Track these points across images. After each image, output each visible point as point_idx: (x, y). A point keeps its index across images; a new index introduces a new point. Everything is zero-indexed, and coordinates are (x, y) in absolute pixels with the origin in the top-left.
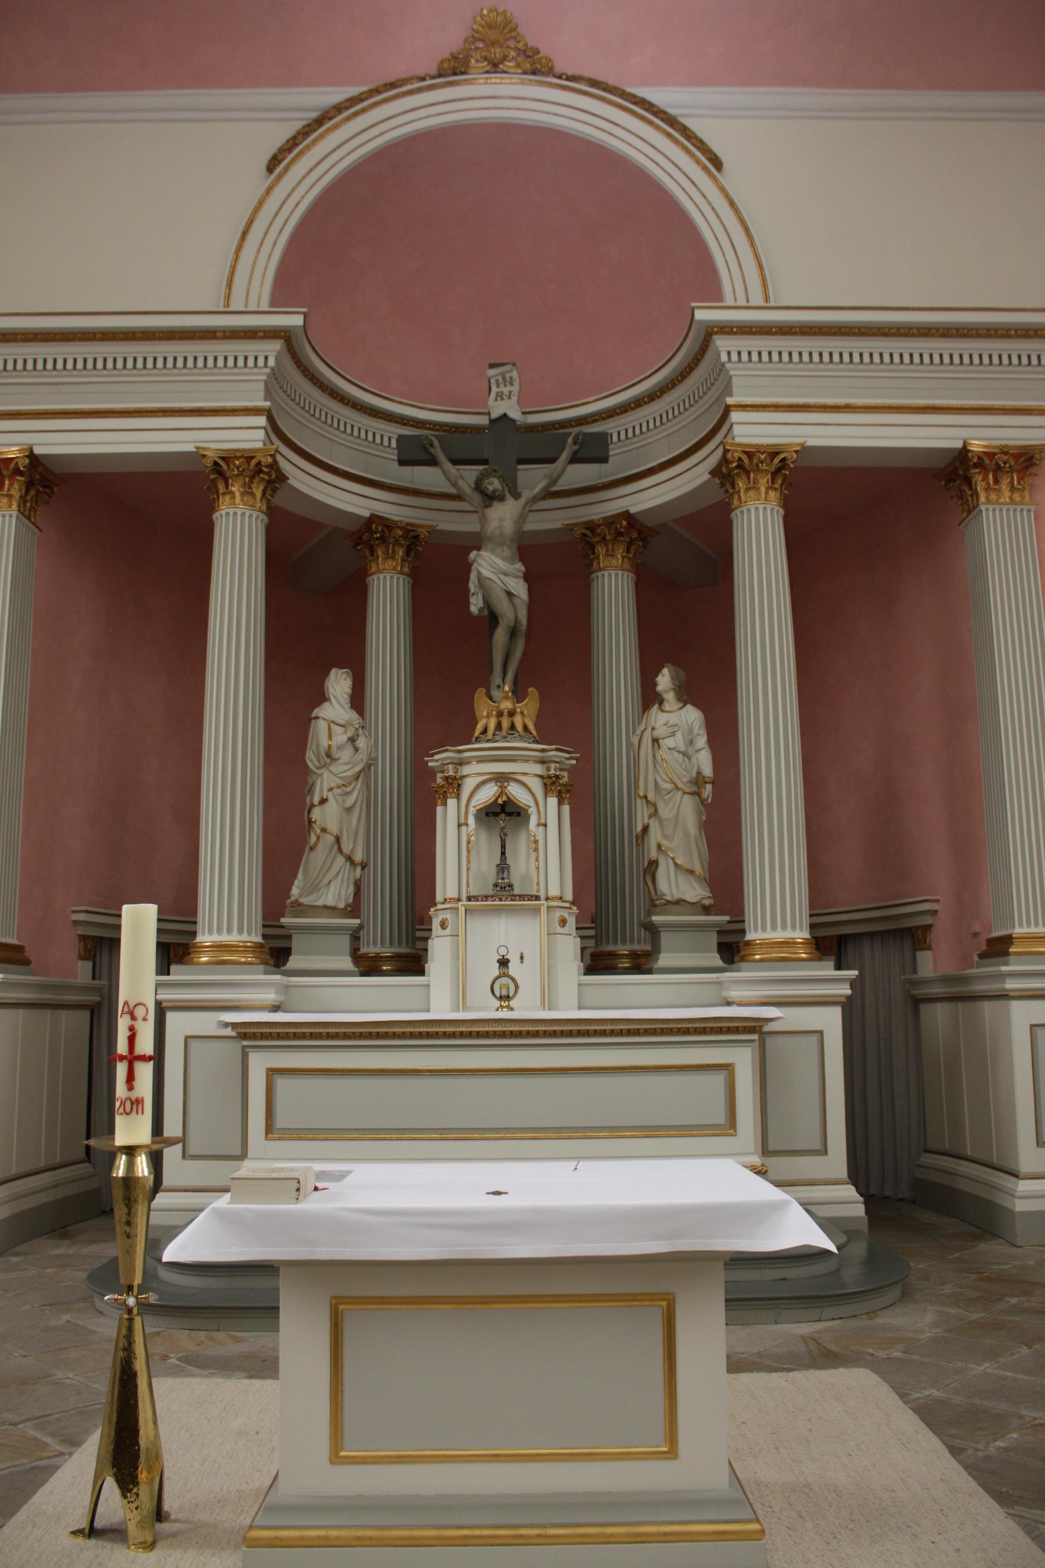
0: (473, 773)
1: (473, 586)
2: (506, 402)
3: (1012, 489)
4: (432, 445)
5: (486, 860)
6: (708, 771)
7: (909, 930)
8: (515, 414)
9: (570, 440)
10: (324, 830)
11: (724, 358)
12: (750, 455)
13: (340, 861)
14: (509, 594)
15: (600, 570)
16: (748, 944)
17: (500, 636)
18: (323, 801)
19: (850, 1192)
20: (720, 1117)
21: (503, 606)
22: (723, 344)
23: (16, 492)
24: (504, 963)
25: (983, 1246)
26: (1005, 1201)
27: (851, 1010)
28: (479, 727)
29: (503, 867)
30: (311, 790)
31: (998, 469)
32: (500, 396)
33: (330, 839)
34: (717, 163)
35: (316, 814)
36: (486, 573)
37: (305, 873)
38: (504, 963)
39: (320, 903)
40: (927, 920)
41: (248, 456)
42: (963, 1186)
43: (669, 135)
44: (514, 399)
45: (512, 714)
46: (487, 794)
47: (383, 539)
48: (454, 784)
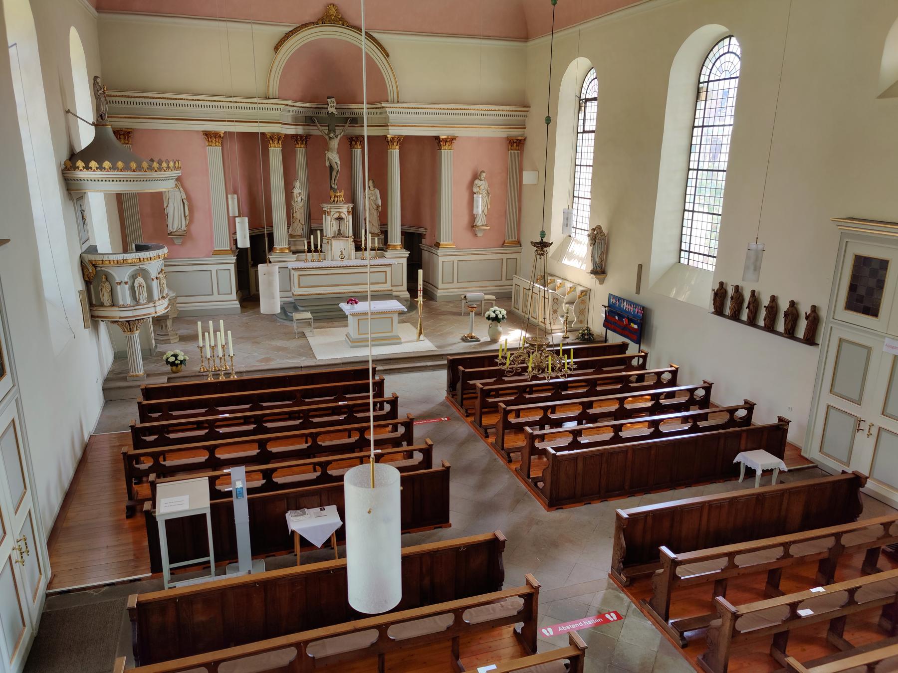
0: (333, 211)
1: (327, 159)
2: (333, 108)
3: (449, 145)
4: (315, 120)
5: (335, 228)
6: (380, 205)
7: (420, 234)
8: (335, 112)
9: (349, 120)
10: (297, 219)
11: (388, 113)
12: (393, 138)
13: (300, 224)
14: (336, 163)
15: (353, 148)
16: (388, 245)
17: (334, 173)
18: (296, 212)
19: (407, 293)
20: (384, 281)
21: (335, 166)
22: (388, 110)
23: (220, 141)
24: (342, 252)
25: (431, 302)
26: (435, 293)
27: (408, 259)
28: (332, 200)
29: (339, 230)
30: (293, 209)
31: (446, 142)
32: (331, 107)
33: (298, 221)
34: (388, 55)
35: (295, 215)
36: (330, 157)
37: (292, 227)
38: (342, 252)
39: (296, 234)
40: (425, 233)
41: (278, 134)
42: (429, 289)
43: (376, 47)
44: (335, 107)
45: (340, 196)
46: (337, 215)
47: (301, 140)
48: (329, 213)
